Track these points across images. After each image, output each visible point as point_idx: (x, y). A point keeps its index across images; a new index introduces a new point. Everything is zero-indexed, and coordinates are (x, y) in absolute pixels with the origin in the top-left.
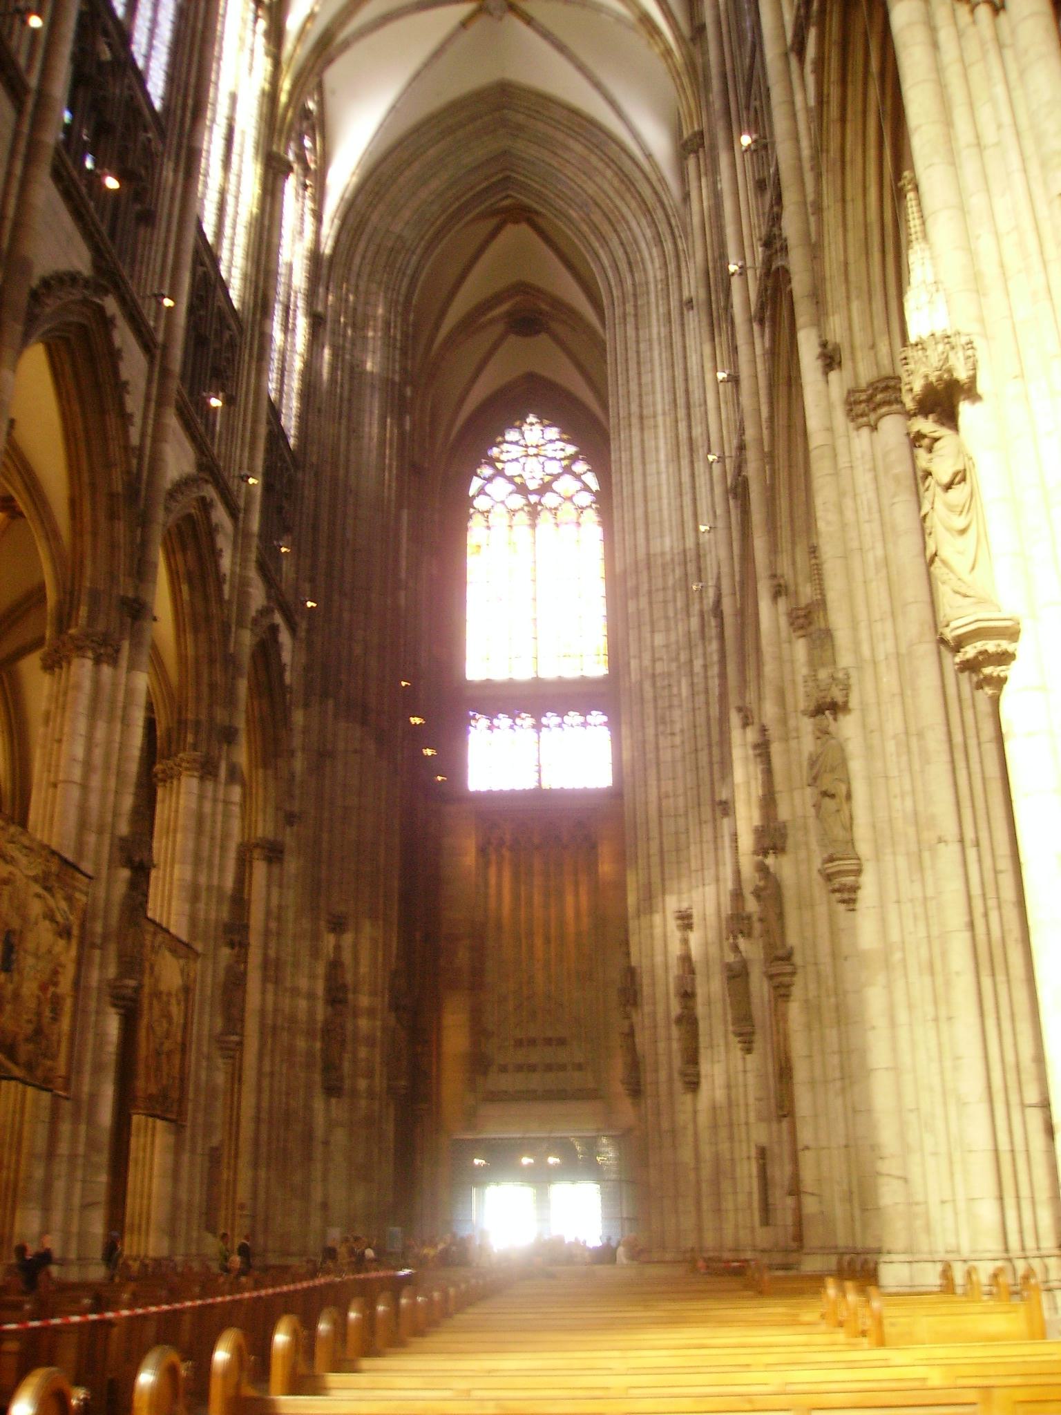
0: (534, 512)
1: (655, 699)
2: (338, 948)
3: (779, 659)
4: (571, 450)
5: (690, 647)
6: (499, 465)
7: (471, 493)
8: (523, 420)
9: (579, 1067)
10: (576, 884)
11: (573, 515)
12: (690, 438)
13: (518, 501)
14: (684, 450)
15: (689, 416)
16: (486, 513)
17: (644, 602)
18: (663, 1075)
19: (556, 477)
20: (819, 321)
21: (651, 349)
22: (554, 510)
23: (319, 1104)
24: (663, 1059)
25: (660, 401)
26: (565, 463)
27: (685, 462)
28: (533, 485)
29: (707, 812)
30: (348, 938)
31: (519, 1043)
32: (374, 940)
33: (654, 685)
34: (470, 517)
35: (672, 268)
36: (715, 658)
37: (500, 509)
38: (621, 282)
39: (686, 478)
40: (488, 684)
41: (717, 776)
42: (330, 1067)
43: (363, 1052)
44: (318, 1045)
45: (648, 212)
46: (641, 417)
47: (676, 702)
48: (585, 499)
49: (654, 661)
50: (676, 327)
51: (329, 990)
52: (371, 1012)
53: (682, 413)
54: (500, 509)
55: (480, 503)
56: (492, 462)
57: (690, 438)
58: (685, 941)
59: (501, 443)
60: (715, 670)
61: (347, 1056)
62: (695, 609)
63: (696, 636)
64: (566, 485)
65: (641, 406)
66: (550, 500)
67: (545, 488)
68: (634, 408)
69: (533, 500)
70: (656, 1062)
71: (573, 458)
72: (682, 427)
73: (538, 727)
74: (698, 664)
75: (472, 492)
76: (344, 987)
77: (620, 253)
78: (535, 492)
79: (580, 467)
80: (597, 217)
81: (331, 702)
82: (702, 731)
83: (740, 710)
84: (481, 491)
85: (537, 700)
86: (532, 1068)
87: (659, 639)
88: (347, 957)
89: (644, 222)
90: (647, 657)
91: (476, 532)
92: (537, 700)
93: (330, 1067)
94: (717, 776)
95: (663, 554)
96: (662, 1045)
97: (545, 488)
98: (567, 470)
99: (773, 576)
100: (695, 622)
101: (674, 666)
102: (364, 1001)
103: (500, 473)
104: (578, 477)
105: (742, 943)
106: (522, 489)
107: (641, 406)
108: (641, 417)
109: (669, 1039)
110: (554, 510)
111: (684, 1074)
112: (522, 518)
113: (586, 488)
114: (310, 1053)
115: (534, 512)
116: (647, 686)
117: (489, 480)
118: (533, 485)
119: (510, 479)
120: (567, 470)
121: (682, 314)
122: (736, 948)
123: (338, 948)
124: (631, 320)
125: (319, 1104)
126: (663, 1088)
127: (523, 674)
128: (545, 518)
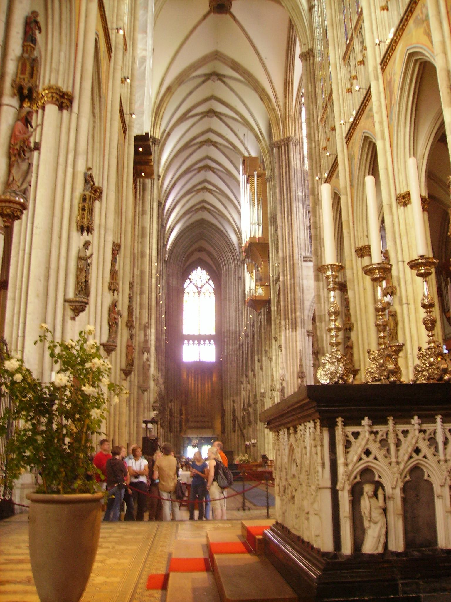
0: (199, 293)
3: (252, 380)
4: (209, 277)
5: (237, 351)
10: (208, 382)
20: (258, 355)
23: (169, 434)
25: (233, 297)
27: (237, 313)
28: (199, 286)
29: (239, 383)
30: (173, 404)
31: (195, 416)
42: (170, 427)
45: (232, 253)
56: (190, 279)
64: (207, 286)
66: (203, 290)
67: (202, 287)
69: (199, 289)
71: (209, 280)
72: (237, 304)
73: (199, 344)
74: (238, 354)
75: (185, 286)
79: (211, 282)
85: (199, 339)
86: (198, 422)
91: (186, 297)
92: (199, 339)
93: (170, 427)
97: (202, 287)
98: (207, 282)
100: (238, 346)
102: (176, 415)
103: (191, 282)
112: (197, 294)
115: (199, 293)
118: (199, 286)
120: (207, 282)
125: (169, 434)
127: (197, 333)
128: (202, 294)
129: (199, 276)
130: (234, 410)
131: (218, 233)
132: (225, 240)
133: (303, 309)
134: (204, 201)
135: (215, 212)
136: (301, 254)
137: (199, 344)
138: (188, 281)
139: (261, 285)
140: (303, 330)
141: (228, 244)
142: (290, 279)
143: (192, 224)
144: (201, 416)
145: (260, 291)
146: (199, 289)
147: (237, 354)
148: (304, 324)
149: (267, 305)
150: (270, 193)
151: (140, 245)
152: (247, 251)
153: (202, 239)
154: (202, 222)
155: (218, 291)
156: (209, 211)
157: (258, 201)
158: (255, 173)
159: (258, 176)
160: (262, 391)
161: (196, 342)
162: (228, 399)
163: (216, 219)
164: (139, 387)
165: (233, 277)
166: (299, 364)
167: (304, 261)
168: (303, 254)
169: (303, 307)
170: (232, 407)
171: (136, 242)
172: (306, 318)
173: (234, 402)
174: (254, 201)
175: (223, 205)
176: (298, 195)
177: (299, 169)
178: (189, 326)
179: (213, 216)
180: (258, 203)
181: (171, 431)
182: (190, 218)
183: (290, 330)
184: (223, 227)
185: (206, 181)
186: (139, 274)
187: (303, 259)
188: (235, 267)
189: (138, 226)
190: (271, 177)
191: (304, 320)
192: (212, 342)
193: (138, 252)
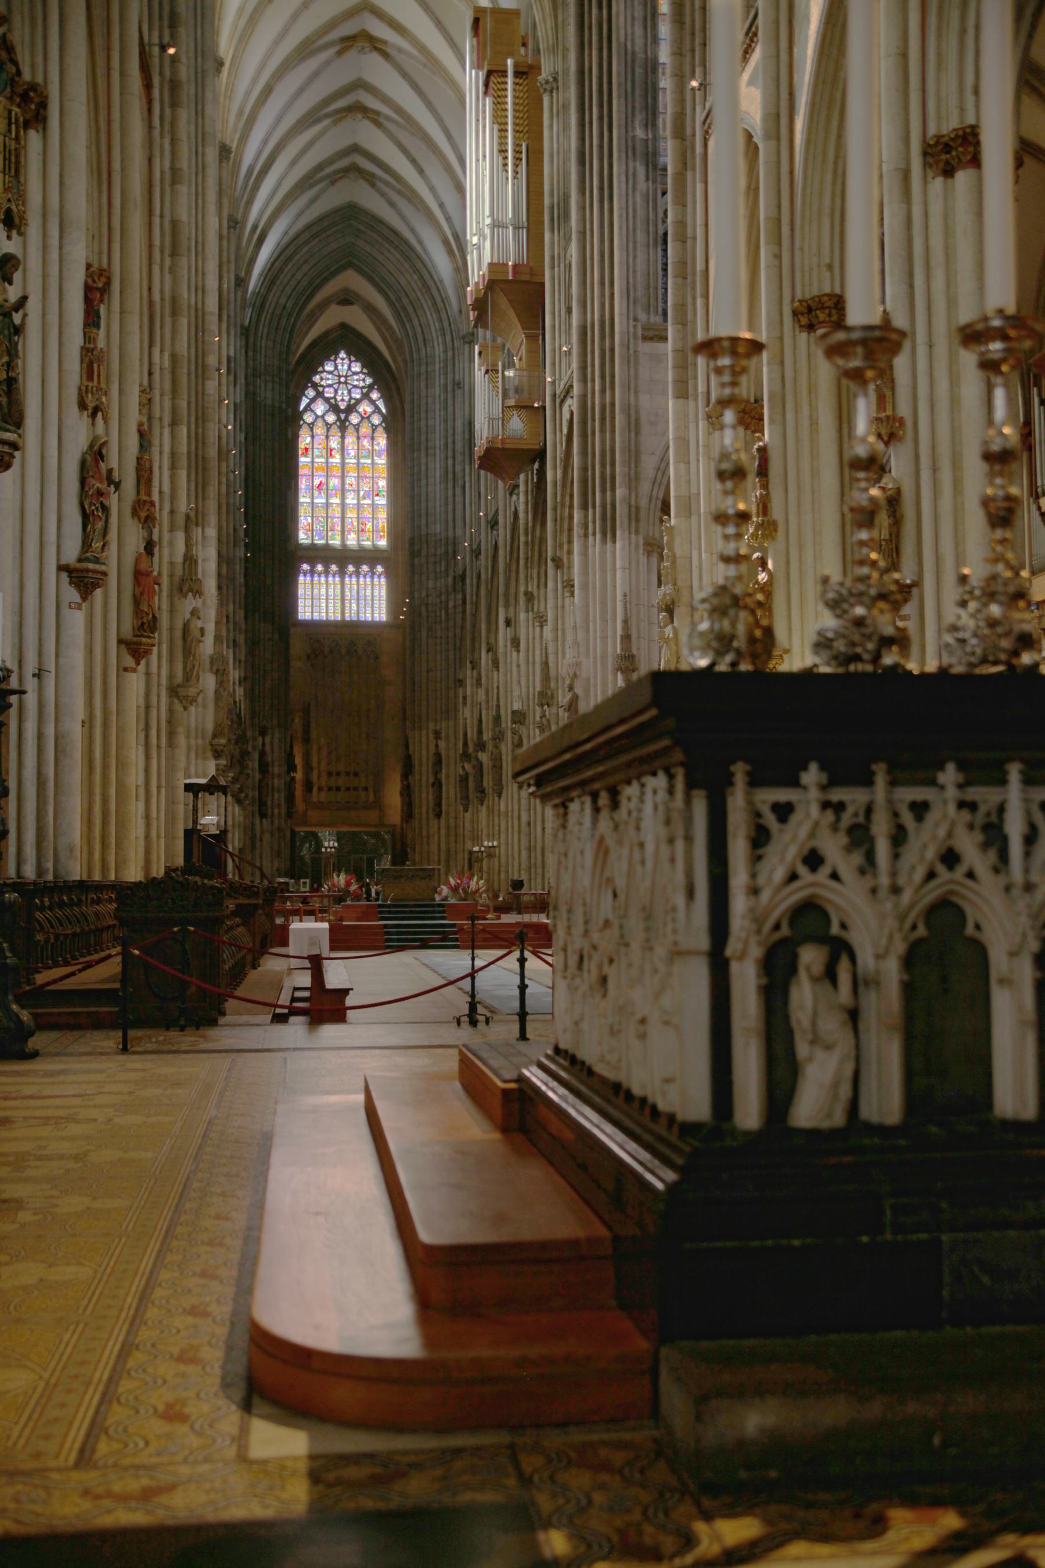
0: (343, 426)
1: (428, 617)
2: (264, 744)
3: (487, 676)
5: (448, 594)
6: (321, 389)
7: (302, 408)
8: (337, 354)
9: (366, 789)
11: (369, 431)
12: (454, 473)
13: (331, 418)
14: (450, 476)
15: (454, 458)
16: (311, 426)
17: (423, 560)
18: (424, 809)
19: (358, 402)
20: (507, 606)
21: (434, 403)
22: (357, 427)
24: (424, 802)
25: (437, 439)
26: (365, 391)
27: (450, 485)
28: (343, 406)
30: (268, 739)
32: (280, 739)
33: (427, 610)
34: (300, 426)
35: (450, 354)
36: (460, 602)
37: (320, 423)
38: (419, 350)
39: (450, 494)
40: (313, 547)
41: (458, 666)
42: (262, 804)
43: (276, 796)
44: (257, 794)
45: (438, 311)
46: (427, 448)
47: (438, 620)
48: (376, 420)
49: (427, 596)
50: (450, 395)
51: (260, 766)
52: (279, 776)
53: (450, 454)
54: (320, 423)
55: (308, 418)
57: (454, 473)
58: (437, 746)
59: (322, 372)
60: (460, 609)
61: (270, 798)
62: (451, 573)
63: (450, 589)
64: (365, 408)
65: (427, 440)
66: (354, 419)
67: (351, 409)
68: (423, 438)
69: (343, 414)
70: (421, 803)
71: (370, 388)
72: (450, 462)
73: (342, 573)
74: (451, 604)
76: (267, 765)
77: (419, 330)
78: (343, 411)
80: (405, 301)
81: (257, 615)
82: (451, 641)
83: (471, 662)
84: (308, 408)
85: (342, 559)
87: (431, 584)
88: (268, 749)
89: (435, 316)
90: (424, 594)
91: (304, 440)
92: (342, 559)
93: (262, 804)
94: (458, 666)
95: (435, 535)
96: (424, 796)
98: (366, 396)
99: (488, 644)
100: (450, 580)
101: (438, 600)
102: (276, 770)
103: (320, 395)
104: (373, 402)
105: (466, 765)
106: (334, 408)
107: (427, 440)
108: (427, 448)
109: (428, 793)
110: (357, 427)
111: (434, 810)
113: (377, 410)
114: (253, 798)
115: (343, 426)
116: (423, 608)
117: (313, 400)
118: (343, 406)
119: (327, 400)
121: (454, 390)
122: (463, 768)
123: (264, 744)
124: (423, 377)
126: (424, 816)
128: (350, 430)
129: (342, 376)
130: (438, 756)
131: (396, 247)
132: (416, 271)
133: (637, 478)
134: (355, 149)
135: (387, 184)
136: (635, 319)
137: (342, 573)
138: (311, 393)
139: (519, 407)
140: (633, 536)
141: (425, 284)
142: (603, 391)
143: (321, 219)
144: (348, 774)
145: (517, 424)
146: (343, 414)
147: (447, 602)
148: (637, 520)
149: (536, 466)
150: (551, 126)
151: (168, 278)
152: (480, 305)
153: (350, 265)
154: (350, 215)
155: (397, 423)
156: (370, 179)
157: (517, 152)
158: (510, 62)
159: (517, 74)
160: (516, 706)
161: (334, 568)
162: (420, 729)
163: (392, 204)
164: (173, 691)
165: (438, 381)
166: (619, 632)
167: (645, 338)
168: (642, 316)
169: (637, 474)
170: (432, 749)
171: (156, 269)
172: (643, 503)
173: (437, 735)
174: (503, 151)
175: (413, 161)
176: (634, 137)
177: (640, 55)
178: (313, 520)
179: (383, 195)
180: (517, 159)
181: (263, 815)
182: (314, 200)
183: (598, 536)
184: (413, 231)
185: (359, 84)
186: (167, 364)
187: (640, 332)
188: (445, 351)
189: (162, 216)
190: (555, 79)
191: (638, 508)
192: (379, 569)
193: (162, 299)
